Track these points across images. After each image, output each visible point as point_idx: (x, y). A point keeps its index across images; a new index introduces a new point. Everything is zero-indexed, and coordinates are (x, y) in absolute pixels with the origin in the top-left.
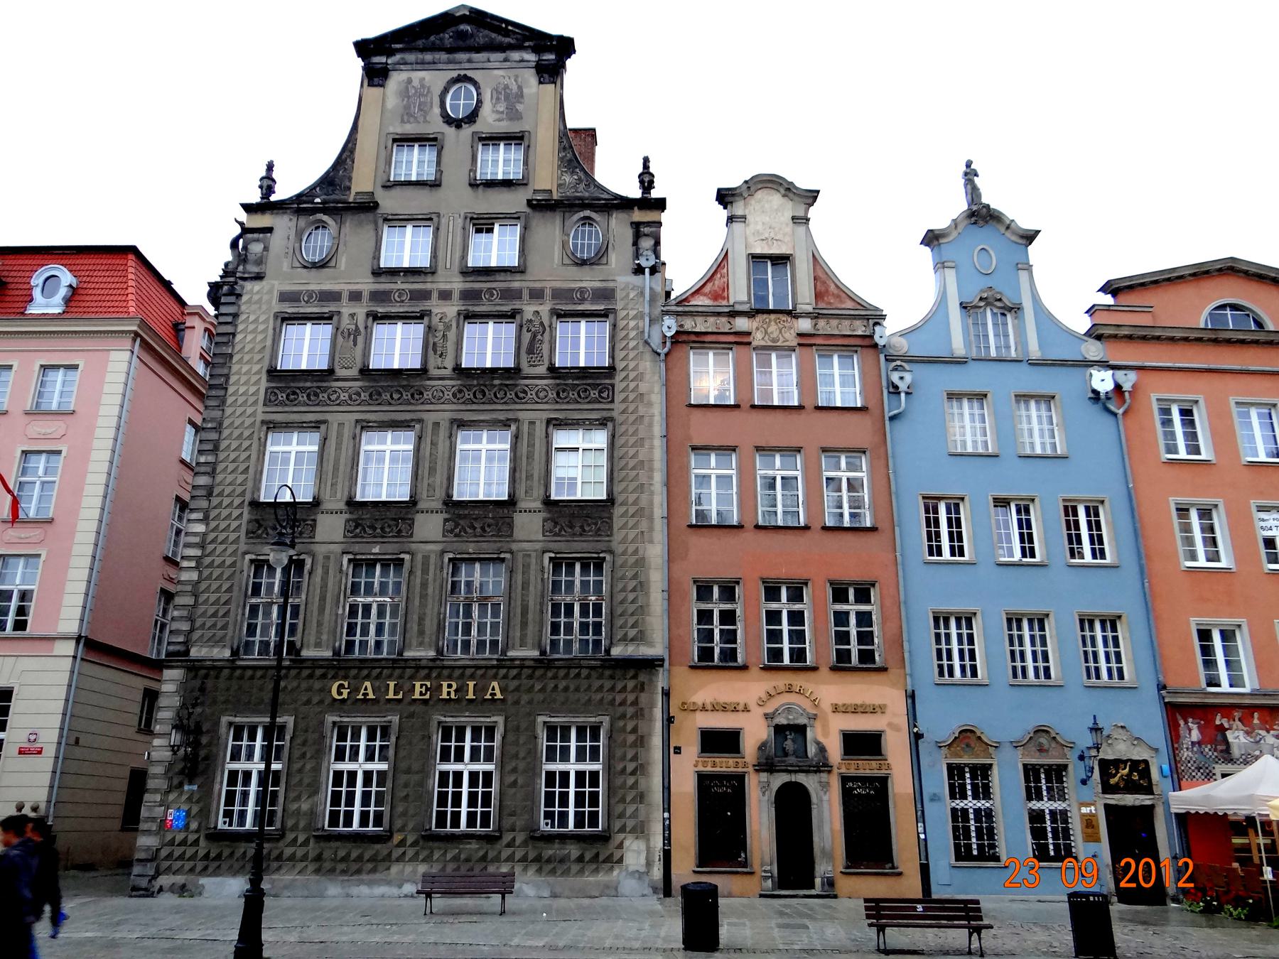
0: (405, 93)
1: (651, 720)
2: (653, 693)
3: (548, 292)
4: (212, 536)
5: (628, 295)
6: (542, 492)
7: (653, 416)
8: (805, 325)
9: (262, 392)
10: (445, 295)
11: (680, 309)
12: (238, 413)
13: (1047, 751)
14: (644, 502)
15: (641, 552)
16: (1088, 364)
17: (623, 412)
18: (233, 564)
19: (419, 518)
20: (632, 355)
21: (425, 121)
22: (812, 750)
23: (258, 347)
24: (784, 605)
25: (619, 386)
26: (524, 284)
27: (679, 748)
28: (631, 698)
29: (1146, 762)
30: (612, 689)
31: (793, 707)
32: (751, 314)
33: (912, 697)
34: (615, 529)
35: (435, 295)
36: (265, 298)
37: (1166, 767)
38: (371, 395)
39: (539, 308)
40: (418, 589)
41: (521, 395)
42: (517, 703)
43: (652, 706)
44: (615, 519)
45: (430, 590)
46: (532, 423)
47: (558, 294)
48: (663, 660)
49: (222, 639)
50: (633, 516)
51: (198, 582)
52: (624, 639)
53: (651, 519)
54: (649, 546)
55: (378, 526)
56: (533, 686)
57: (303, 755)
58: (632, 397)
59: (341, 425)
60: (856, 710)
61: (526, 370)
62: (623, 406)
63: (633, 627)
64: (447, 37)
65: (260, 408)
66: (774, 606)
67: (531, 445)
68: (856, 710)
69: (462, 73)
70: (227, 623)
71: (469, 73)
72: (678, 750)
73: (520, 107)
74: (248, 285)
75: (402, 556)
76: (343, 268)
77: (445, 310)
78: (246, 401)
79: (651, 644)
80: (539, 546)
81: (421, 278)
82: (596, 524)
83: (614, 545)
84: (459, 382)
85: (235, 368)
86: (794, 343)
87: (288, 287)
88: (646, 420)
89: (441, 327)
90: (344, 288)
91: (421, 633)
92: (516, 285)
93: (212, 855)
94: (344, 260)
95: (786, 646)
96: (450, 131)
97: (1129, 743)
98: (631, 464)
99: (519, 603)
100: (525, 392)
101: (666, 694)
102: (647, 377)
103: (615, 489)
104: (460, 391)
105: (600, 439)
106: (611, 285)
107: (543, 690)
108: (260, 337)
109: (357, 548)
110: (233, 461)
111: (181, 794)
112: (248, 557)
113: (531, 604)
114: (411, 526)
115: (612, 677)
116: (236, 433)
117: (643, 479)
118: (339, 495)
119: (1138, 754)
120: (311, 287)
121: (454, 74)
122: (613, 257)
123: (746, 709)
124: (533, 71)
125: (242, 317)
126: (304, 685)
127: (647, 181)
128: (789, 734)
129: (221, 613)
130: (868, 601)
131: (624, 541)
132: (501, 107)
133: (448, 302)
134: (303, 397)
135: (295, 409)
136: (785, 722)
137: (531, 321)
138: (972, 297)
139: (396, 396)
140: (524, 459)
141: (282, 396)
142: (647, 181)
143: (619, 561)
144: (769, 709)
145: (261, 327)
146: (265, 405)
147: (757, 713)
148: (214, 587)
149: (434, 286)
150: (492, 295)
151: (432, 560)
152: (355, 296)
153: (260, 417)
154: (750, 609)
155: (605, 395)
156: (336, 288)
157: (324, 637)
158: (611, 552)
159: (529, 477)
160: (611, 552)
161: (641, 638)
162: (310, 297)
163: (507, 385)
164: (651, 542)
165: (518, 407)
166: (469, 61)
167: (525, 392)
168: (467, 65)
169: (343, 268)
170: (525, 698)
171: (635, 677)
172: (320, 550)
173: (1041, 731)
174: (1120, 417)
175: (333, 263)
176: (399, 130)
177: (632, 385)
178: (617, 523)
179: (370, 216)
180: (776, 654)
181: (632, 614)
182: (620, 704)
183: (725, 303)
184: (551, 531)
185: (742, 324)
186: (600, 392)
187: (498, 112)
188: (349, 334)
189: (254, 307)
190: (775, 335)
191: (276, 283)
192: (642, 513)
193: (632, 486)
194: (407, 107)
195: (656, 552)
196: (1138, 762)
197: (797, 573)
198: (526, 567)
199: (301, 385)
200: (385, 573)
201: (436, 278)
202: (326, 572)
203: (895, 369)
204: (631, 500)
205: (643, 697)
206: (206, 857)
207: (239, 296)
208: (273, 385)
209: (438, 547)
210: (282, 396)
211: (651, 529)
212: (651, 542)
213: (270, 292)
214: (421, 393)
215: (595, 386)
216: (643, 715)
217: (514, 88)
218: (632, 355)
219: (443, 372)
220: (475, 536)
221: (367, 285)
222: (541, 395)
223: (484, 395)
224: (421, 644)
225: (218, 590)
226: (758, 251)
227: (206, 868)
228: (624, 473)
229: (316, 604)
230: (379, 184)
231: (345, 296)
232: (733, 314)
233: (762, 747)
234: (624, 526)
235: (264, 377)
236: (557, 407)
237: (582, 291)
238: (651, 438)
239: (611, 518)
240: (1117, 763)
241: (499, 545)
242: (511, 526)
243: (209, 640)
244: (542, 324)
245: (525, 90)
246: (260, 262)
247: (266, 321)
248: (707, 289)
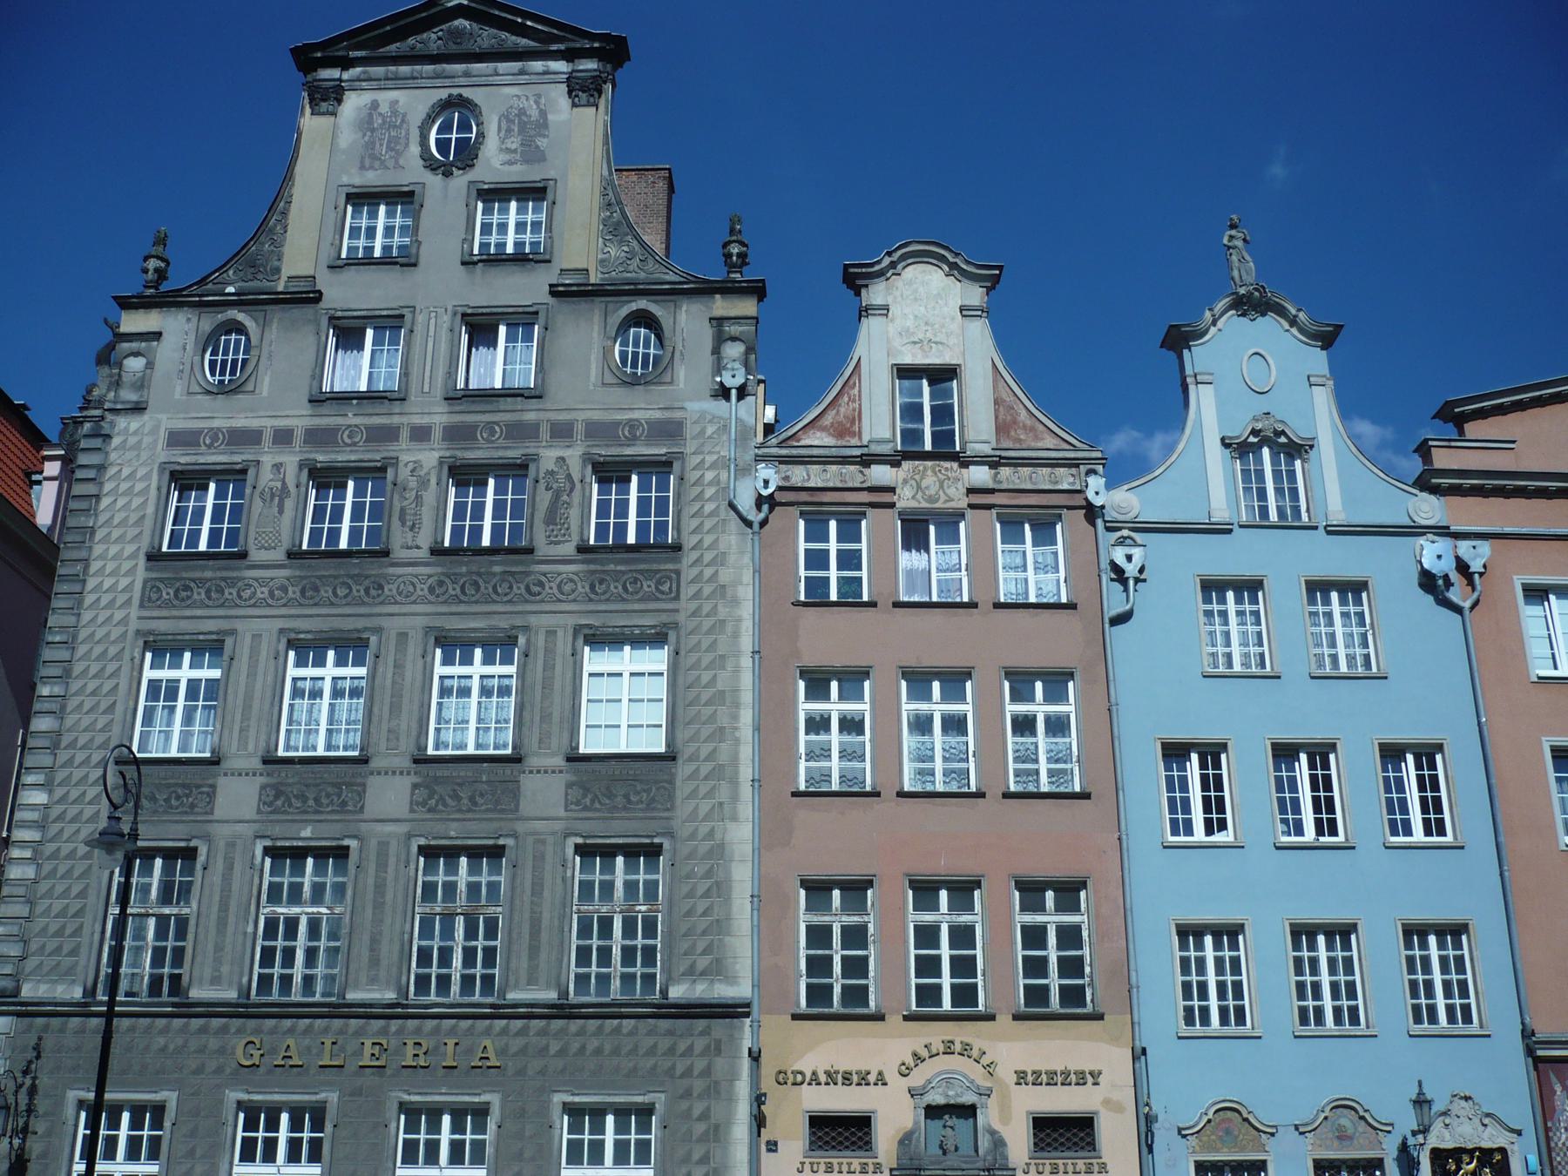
0: (367, 122)
1: (731, 1099)
2: (736, 1056)
3: (579, 428)
4: (56, 811)
5: (703, 431)
6: (565, 741)
7: (739, 620)
8: (980, 475)
9: (138, 586)
10: (421, 434)
11: (784, 452)
12: (100, 619)
13: (1350, 1138)
14: (723, 757)
15: (718, 836)
16: (1413, 530)
17: (694, 614)
19: (374, 783)
20: (708, 525)
21: (398, 166)
22: (984, 1143)
23: (133, 518)
24: (943, 914)
25: (688, 574)
26: (542, 415)
27: (776, 1144)
28: (700, 1064)
29: (1502, 1151)
30: (671, 1051)
31: (951, 1077)
32: (894, 460)
33: (1139, 1054)
34: (678, 801)
35: (405, 434)
36: (147, 440)
37: (1533, 1160)
38: (303, 592)
39: (566, 453)
40: (370, 896)
41: (536, 589)
42: (521, 1072)
43: (733, 1077)
44: (678, 783)
45: (389, 896)
46: (551, 633)
47: (596, 431)
48: (748, 1005)
49: (70, 971)
50: (706, 778)
51: (35, 881)
52: (691, 973)
53: (734, 783)
54: (730, 825)
55: (311, 796)
56: (546, 1048)
57: (191, 1153)
58: (707, 590)
59: (257, 637)
60: (1051, 1079)
61: (543, 549)
62: (693, 605)
63: (704, 953)
64: (432, 40)
65: (134, 612)
66: (928, 918)
67: (549, 667)
68: (1051, 1079)
69: (455, 91)
70: (79, 945)
71: (466, 93)
72: (772, 1146)
73: (542, 143)
74: (122, 422)
75: (346, 842)
76: (265, 394)
77: (420, 456)
78: (114, 600)
79: (732, 980)
80: (559, 826)
81: (385, 407)
82: (648, 791)
83: (676, 824)
84: (439, 570)
85: (98, 550)
86: (963, 503)
87: (181, 425)
88: (729, 628)
89: (413, 483)
90: (265, 423)
91: (375, 962)
92: (530, 416)
94: (267, 380)
95: (946, 981)
96: (434, 181)
97: (1476, 1121)
98: (704, 697)
99: (527, 915)
100: (541, 584)
101: (755, 1057)
102: (732, 559)
103: (680, 736)
104: (441, 583)
105: (656, 659)
106: (677, 415)
107: (562, 1052)
108: (137, 502)
109: (277, 830)
110: (93, 693)
113: (546, 916)
114: (361, 795)
115: (670, 1033)
116: (98, 650)
117: (723, 720)
118: (251, 747)
119: (1491, 1138)
120: (216, 424)
121: (443, 94)
122: (681, 373)
123: (881, 1080)
124: (564, 87)
125: (112, 471)
126: (194, 1044)
129: (68, 932)
130: (1075, 908)
131: (693, 816)
132: (514, 143)
133: (425, 445)
134: (199, 595)
135: (188, 613)
136: (941, 1100)
137: (552, 473)
138: (1240, 430)
139: (341, 592)
140: (539, 688)
141: (167, 593)
143: (684, 850)
144: (917, 1078)
145: (139, 486)
146: (142, 606)
147: (898, 1085)
148: (59, 889)
149: (405, 420)
150: (493, 432)
151: (393, 849)
152: (283, 437)
153: (134, 624)
154: (892, 920)
155: (666, 588)
156: (254, 423)
157: (225, 969)
158: (670, 834)
159: (546, 717)
160: (670, 834)
161: (718, 970)
162: (215, 438)
163: (512, 574)
164: (734, 818)
165: (529, 607)
166: (467, 74)
167: (541, 584)
168: (463, 81)
169: (265, 394)
170: (535, 1065)
171: (706, 1032)
172: (222, 832)
173: (1341, 1106)
174: (1467, 612)
175: (250, 387)
176: (357, 181)
177: (708, 572)
178: (682, 789)
179: (308, 310)
180: (929, 995)
181: (704, 933)
182: (682, 1076)
183: (855, 441)
184: (578, 803)
185: (881, 474)
186: (659, 583)
187: (508, 151)
188: (273, 496)
189: (129, 455)
190: (932, 492)
191: (163, 417)
192: (724, 773)
193: (706, 731)
194: (370, 145)
195: (741, 834)
196: (1491, 1151)
197: (963, 867)
198: (539, 858)
199: (198, 574)
200: (319, 870)
201: (407, 407)
202: (230, 867)
203: (1121, 542)
204: (703, 754)
205: (720, 1063)
207: (108, 437)
208: (154, 575)
209: (402, 829)
210: (167, 593)
211: (735, 798)
212: (734, 818)
213: (154, 431)
214: (381, 587)
215: (649, 574)
216: (718, 1093)
217: (534, 113)
218: (708, 525)
219: (415, 553)
220: (460, 811)
221: (300, 418)
222: (567, 588)
223: (478, 589)
224: (373, 980)
225: (65, 894)
226: (909, 358)
228: (693, 710)
229: (214, 917)
230: (324, 262)
231: (267, 437)
232: (866, 461)
233: (906, 1140)
234: (693, 795)
235: (142, 561)
236: (592, 607)
237: (633, 425)
238: (737, 654)
239: (671, 782)
240: (1457, 1153)
241: (495, 825)
242: (515, 794)
244: (569, 477)
245: (550, 117)
246: (141, 384)
247: (147, 476)
248: (828, 420)
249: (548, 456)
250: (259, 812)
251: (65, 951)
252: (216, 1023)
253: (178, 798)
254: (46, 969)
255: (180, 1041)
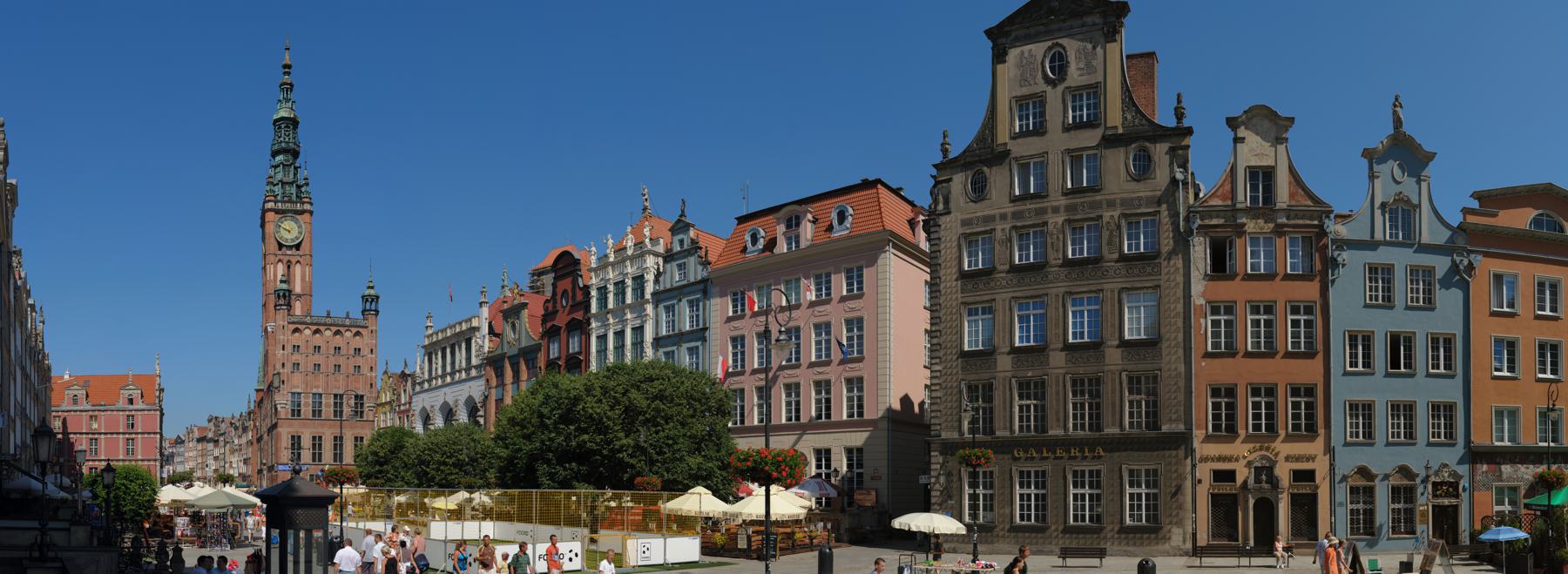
10: (1056, 210)
47: (1124, 202)
127: (1179, 115)
128: (1265, 472)
142: (1179, 115)
178: (1164, 353)
237: (1139, 199)
249: (1107, 215)
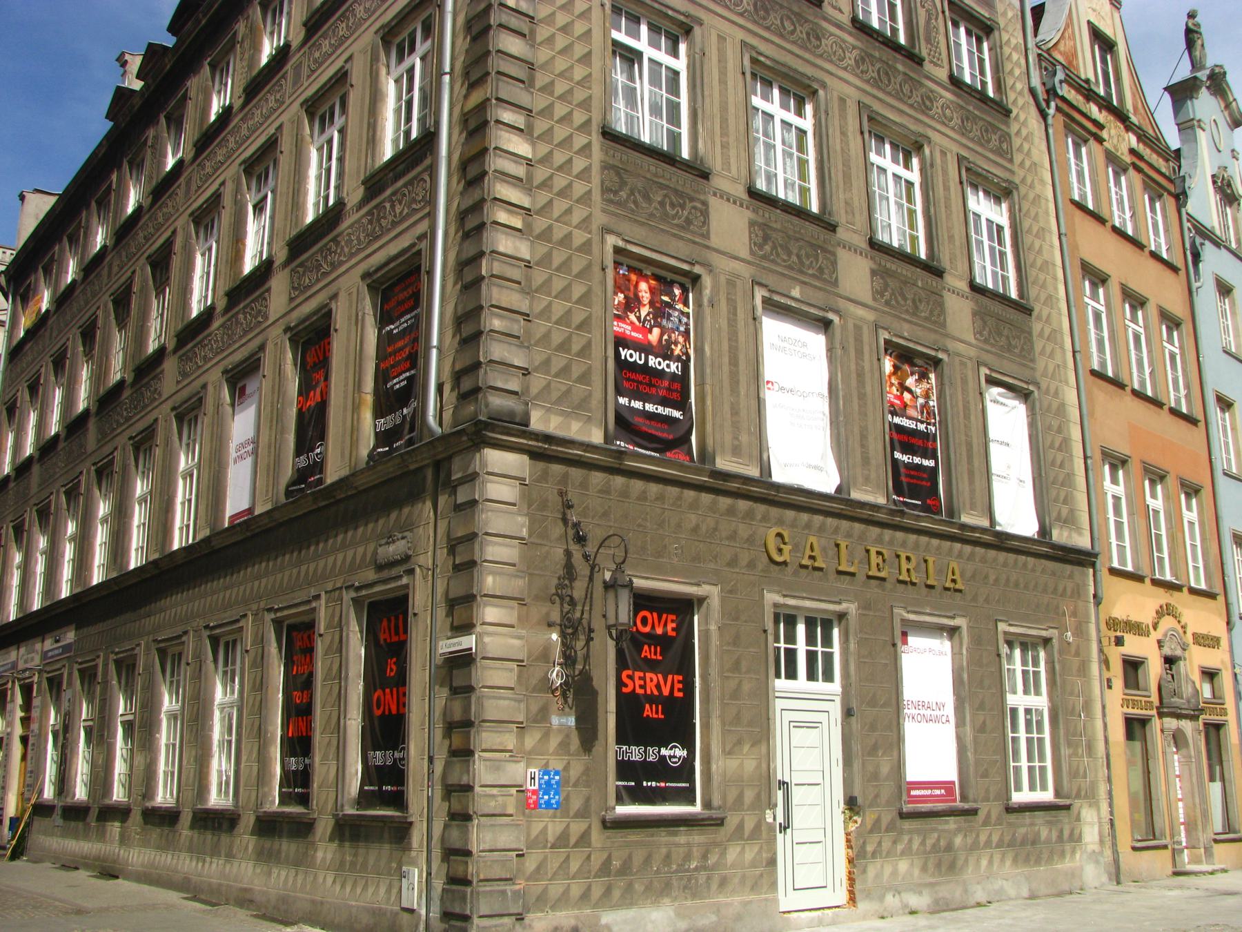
18: (586, 247)
93: (616, 863)
111: (546, 735)
112: (611, 240)
129: (576, 347)
139: (789, 26)
206: (605, 869)
225: (564, 293)
227: (608, 891)
243: (559, 401)
250: (752, 253)
251: (575, 375)
252: (743, 505)
253: (673, 205)
254: (555, 395)
255: (711, 522)
